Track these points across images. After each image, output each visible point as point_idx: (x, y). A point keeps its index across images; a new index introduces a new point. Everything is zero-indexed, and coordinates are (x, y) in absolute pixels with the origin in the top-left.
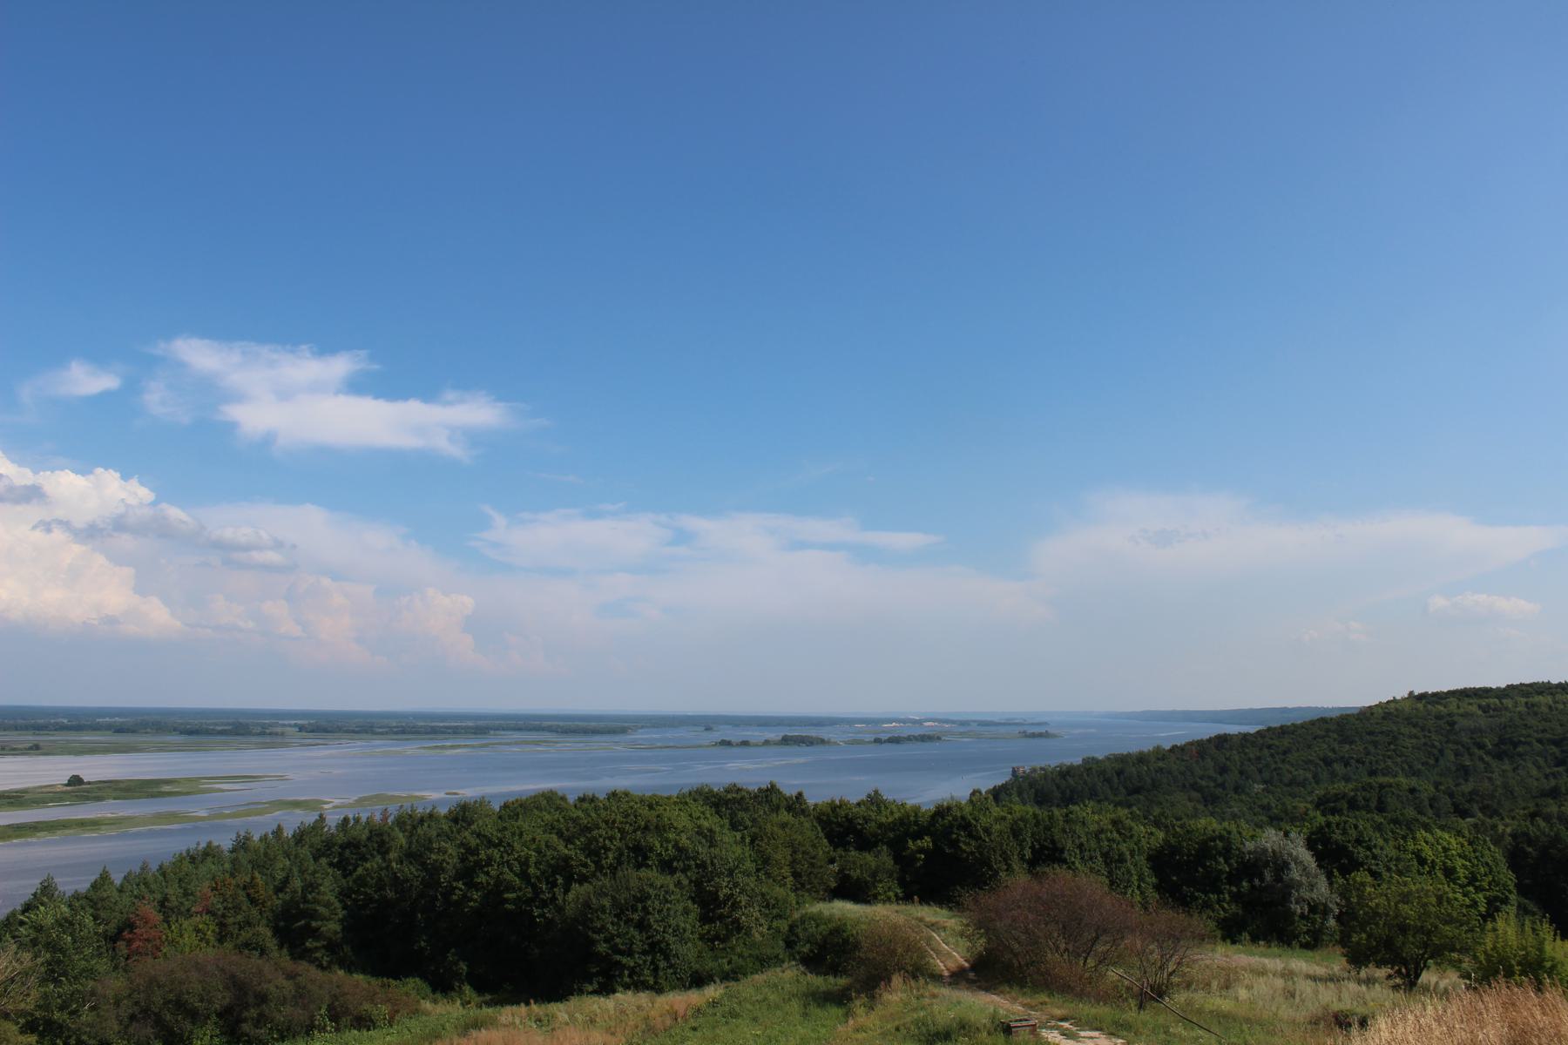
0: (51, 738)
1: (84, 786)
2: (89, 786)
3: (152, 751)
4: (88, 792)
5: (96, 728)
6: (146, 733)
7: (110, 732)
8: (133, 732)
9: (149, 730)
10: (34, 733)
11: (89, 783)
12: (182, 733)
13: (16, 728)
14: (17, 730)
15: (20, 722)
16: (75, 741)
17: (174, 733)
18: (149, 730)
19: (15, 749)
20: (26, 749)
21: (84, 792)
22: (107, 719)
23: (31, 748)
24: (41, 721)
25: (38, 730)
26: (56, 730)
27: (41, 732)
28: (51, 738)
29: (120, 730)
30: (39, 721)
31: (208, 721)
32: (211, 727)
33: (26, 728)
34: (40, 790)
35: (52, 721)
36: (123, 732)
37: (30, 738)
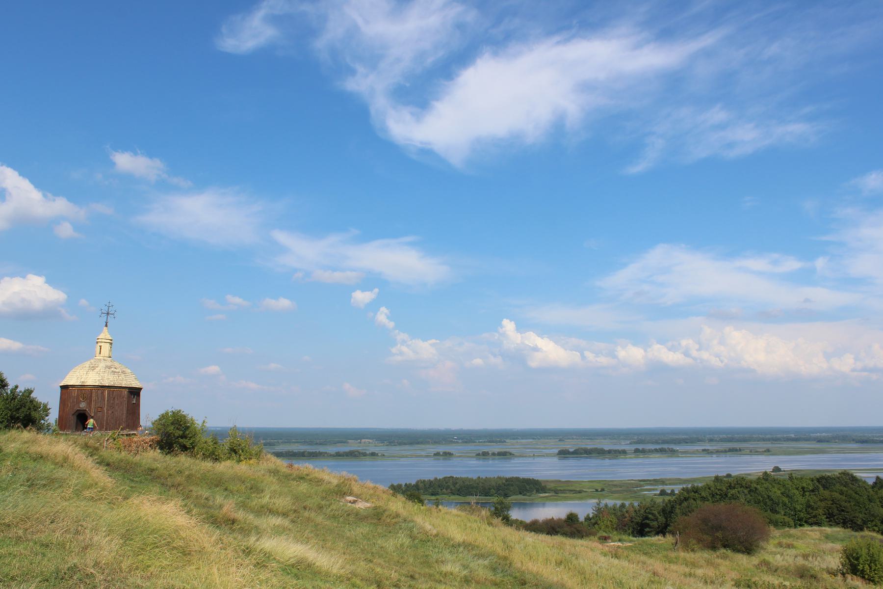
0: (781, 445)
1: (781, 473)
2: (783, 473)
3: (835, 453)
4: (782, 476)
5: (808, 440)
6: (836, 442)
7: (813, 442)
8: (828, 442)
9: (837, 441)
10: (772, 443)
11: (784, 471)
12: (857, 442)
13: (764, 440)
14: (764, 441)
15: (768, 436)
16: (793, 447)
17: (852, 442)
18: (837, 441)
19: (757, 452)
20: (763, 452)
21: (780, 476)
22: (818, 434)
23: (765, 451)
24: (779, 436)
25: (776, 441)
26: (785, 441)
27: (776, 442)
28: (781, 445)
29: (820, 441)
30: (778, 436)
31: (878, 435)
32: (878, 439)
33: (769, 440)
34: (757, 474)
35: (785, 436)
36: (822, 442)
37: (768, 445)
